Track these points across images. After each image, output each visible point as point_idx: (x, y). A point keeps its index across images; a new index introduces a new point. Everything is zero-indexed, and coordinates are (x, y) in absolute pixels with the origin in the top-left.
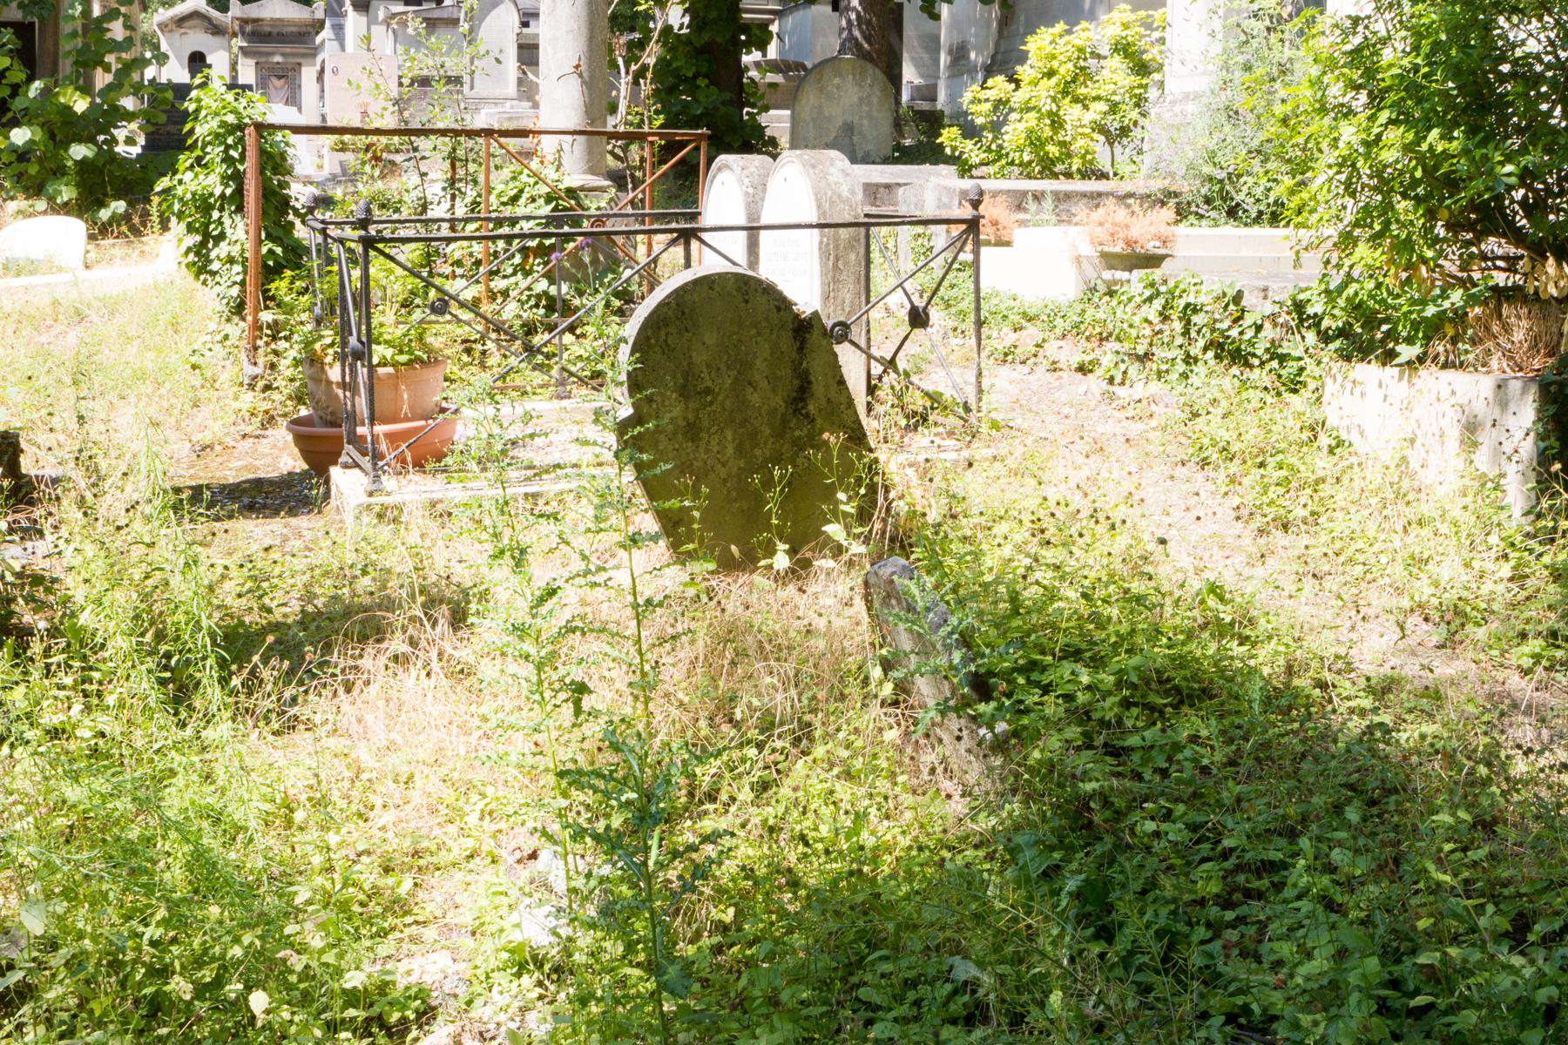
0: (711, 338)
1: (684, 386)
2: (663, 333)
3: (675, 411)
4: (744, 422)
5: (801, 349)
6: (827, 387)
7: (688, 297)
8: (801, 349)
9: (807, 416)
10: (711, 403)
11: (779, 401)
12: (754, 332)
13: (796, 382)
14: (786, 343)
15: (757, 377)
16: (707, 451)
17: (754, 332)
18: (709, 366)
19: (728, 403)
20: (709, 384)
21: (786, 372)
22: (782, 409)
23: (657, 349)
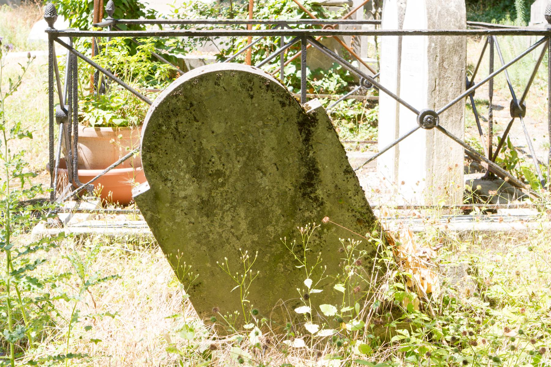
0: (219, 127)
1: (197, 168)
2: (173, 121)
3: (189, 189)
4: (256, 202)
5: (307, 140)
6: (334, 175)
7: (195, 91)
8: (307, 140)
9: (316, 199)
10: (223, 184)
11: (288, 185)
12: (260, 123)
13: (304, 170)
14: (292, 134)
15: (266, 163)
16: (221, 226)
17: (260, 123)
18: (218, 152)
19: (239, 185)
20: (220, 167)
21: (293, 160)
22: (292, 192)
23: (168, 135)
